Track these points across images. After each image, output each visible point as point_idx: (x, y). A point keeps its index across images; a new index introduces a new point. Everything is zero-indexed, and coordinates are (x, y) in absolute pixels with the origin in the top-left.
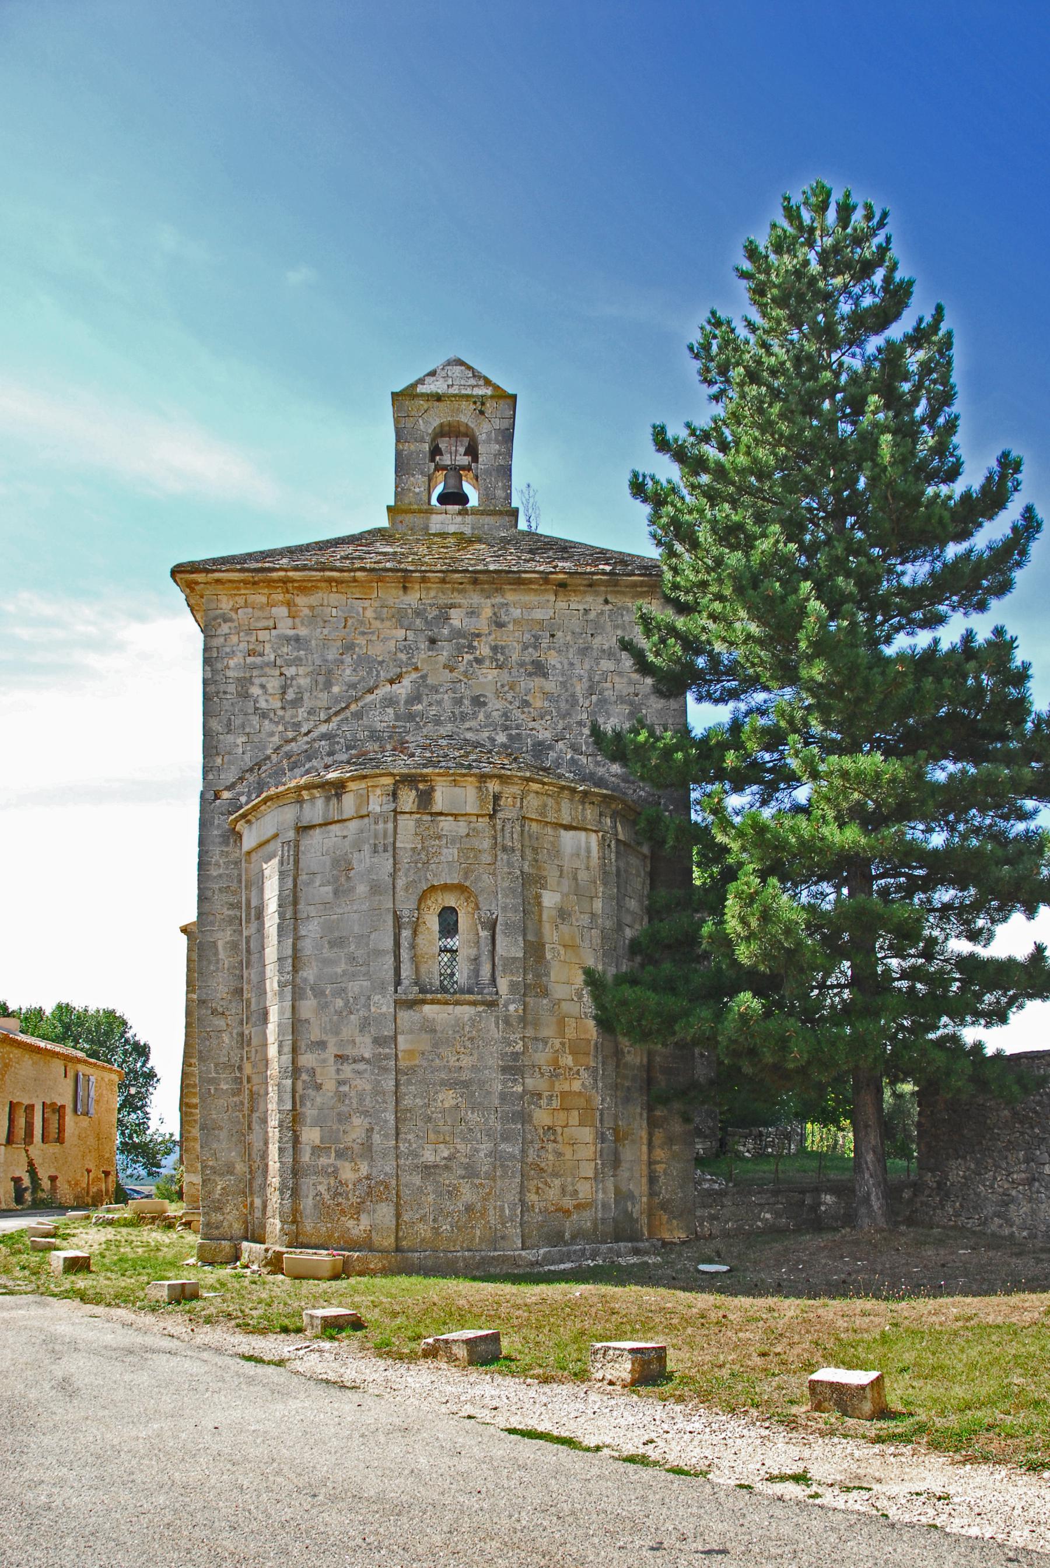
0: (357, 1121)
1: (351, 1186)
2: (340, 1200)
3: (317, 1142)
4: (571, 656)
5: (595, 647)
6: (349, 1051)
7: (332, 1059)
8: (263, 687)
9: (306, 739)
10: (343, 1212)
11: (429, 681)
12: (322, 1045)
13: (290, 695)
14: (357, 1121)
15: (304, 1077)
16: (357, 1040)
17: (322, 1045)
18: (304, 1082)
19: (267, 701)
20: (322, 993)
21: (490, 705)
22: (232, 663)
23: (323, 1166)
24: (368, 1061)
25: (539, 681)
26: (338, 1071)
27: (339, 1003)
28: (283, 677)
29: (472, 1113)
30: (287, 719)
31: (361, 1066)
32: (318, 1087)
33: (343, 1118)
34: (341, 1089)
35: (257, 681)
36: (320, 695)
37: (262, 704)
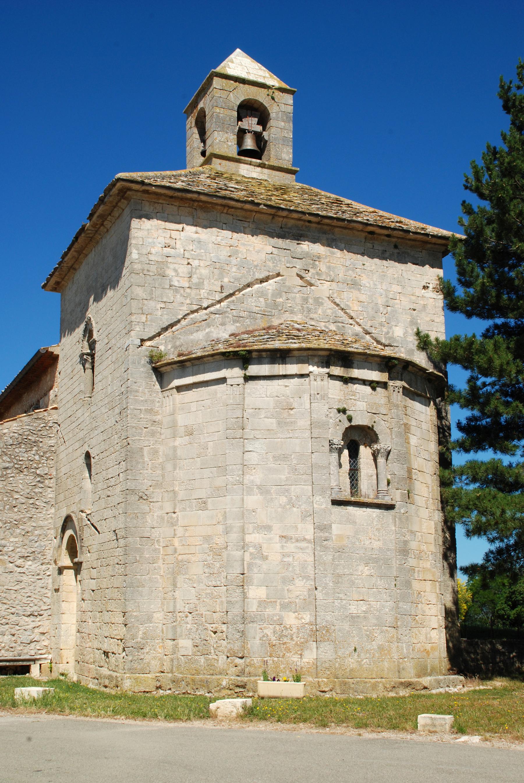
0: (299, 583)
1: (294, 630)
2: (285, 640)
3: (264, 596)
4: (375, 279)
5: (389, 275)
7: (277, 538)
8: (175, 270)
9: (204, 311)
10: (289, 650)
11: (287, 284)
12: (268, 528)
13: (195, 280)
14: (299, 583)
15: (251, 550)
16: (300, 526)
17: (268, 528)
18: (251, 554)
19: (178, 281)
20: (268, 492)
21: (325, 305)
22: (153, 251)
23: (268, 615)
24: (309, 541)
25: (355, 294)
26: (283, 547)
27: (283, 500)
28: (189, 266)
29: (381, 580)
30: (193, 295)
31: (304, 544)
32: (265, 558)
33: (288, 581)
34: (285, 560)
35: (172, 266)
36: (216, 283)
37: (176, 284)
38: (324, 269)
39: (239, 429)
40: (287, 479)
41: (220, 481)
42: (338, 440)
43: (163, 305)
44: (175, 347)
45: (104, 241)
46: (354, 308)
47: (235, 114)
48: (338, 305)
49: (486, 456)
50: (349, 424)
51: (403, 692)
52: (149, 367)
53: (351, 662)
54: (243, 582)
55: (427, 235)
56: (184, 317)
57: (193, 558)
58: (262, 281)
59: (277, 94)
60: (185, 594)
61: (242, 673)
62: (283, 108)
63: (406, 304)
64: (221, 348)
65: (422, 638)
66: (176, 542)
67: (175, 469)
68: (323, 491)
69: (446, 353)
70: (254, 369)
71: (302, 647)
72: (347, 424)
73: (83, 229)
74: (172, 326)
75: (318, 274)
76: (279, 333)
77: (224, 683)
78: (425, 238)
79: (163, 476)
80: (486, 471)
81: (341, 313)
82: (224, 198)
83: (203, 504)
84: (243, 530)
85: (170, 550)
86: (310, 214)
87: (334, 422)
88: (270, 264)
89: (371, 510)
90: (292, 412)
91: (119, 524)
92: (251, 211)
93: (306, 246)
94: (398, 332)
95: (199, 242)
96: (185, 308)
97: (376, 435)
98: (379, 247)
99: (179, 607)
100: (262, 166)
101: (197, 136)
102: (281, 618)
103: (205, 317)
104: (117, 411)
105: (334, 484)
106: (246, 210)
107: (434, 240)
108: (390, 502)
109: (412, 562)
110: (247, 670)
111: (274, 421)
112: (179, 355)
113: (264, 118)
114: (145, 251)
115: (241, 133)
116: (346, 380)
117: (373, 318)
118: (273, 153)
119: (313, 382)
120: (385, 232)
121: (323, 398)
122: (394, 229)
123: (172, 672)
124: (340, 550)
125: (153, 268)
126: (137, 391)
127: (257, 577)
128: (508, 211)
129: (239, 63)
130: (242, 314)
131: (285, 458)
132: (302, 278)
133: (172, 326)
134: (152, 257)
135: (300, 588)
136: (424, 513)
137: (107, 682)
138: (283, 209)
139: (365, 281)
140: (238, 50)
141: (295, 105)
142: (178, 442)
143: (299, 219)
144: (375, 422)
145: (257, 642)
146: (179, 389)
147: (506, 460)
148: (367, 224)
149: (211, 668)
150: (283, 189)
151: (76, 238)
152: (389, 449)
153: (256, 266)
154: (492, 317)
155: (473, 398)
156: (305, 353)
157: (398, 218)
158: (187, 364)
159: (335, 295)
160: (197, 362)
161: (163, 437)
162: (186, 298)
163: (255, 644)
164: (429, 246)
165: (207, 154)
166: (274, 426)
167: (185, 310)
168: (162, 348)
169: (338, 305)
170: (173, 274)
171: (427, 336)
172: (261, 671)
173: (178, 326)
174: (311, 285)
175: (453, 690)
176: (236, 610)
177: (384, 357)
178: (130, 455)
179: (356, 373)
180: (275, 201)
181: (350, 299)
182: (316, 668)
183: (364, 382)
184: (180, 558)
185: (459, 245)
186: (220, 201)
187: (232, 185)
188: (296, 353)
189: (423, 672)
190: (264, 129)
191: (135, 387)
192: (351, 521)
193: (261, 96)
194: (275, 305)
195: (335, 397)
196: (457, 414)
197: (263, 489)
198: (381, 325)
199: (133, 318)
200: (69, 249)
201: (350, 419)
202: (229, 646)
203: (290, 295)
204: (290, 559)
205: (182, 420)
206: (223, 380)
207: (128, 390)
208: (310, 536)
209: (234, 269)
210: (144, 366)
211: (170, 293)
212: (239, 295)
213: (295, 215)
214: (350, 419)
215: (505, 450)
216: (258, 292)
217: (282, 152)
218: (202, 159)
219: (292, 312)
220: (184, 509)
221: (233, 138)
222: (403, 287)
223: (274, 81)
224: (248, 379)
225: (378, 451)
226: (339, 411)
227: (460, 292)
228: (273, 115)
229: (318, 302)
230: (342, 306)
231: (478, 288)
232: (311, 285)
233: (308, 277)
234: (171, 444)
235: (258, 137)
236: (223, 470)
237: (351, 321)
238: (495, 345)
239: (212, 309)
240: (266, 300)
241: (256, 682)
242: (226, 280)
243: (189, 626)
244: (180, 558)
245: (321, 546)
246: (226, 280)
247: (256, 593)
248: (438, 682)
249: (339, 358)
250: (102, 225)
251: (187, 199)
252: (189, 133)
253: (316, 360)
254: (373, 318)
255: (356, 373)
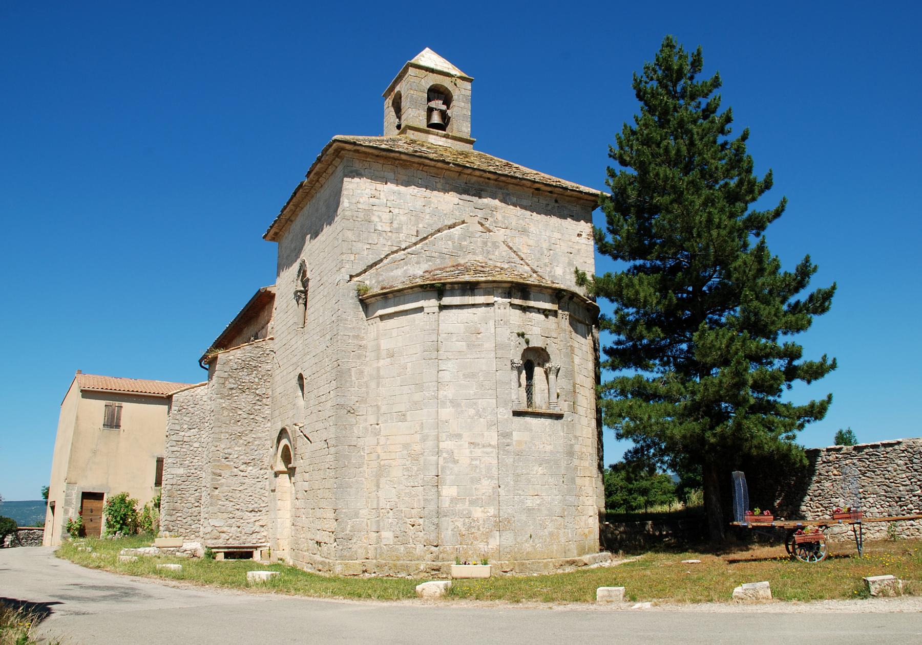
0: (485, 482)
1: (481, 522)
2: (473, 530)
3: (455, 494)
6: (477, 441)
8: (379, 217)
10: (476, 539)
12: (459, 436)
13: (395, 225)
14: (485, 482)
15: (445, 455)
16: (486, 434)
17: (459, 436)
18: (444, 458)
20: (459, 405)
22: (361, 200)
24: (494, 447)
25: (525, 238)
26: (471, 452)
27: (472, 412)
31: (489, 450)
32: (456, 462)
37: (380, 228)
38: (500, 218)
39: (434, 351)
40: (475, 394)
41: (417, 397)
42: (518, 361)
43: (368, 246)
44: (378, 282)
45: (318, 195)
46: (524, 251)
47: (426, 95)
48: (511, 248)
49: (630, 373)
51: (569, 569)
52: (357, 300)
53: (527, 547)
54: (438, 482)
55: (581, 192)
56: (386, 257)
57: (393, 463)
58: (450, 228)
59: (459, 81)
60: (387, 494)
61: (437, 558)
62: (463, 92)
63: (566, 250)
64: (419, 282)
65: (582, 524)
66: (379, 450)
67: (378, 386)
68: (505, 404)
69: (603, 288)
70: (446, 300)
71: (487, 536)
72: (525, 346)
73: (301, 186)
74: (375, 264)
75: (495, 222)
76: (467, 270)
77: (422, 567)
78: (580, 195)
79: (367, 393)
80: (632, 385)
81: (513, 255)
82: (421, 157)
83: (403, 417)
84: (438, 439)
85: (374, 456)
86: (490, 172)
88: (457, 213)
90: (479, 336)
91: (331, 434)
92: (442, 169)
93: (487, 201)
94: (559, 271)
95: (399, 194)
96: (386, 249)
97: (548, 355)
98: (543, 202)
99: (382, 505)
100: (447, 136)
101: (394, 114)
102: (470, 512)
103: (403, 257)
104: (328, 337)
105: (514, 397)
106: (438, 168)
107: (586, 197)
108: (560, 412)
109: (576, 462)
110: (441, 556)
111: (464, 343)
112: (382, 289)
113: (447, 98)
114: (354, 201)
115: (430, 111)
116: (525, 309)
117: (539, 260)
118: (455, 126)
119: (497, 310)
120: (549, 189)
121: (505, 323)
122: (556, 186)
123: (376, 558)
124: (519, 454)
125: (361, 215)
126: (346, 320)
127: (449, 478)
128: (648, 172)
129: (428, 58)
130: (434, 254)
131: (473, 375)
132: (482, 225)
133: (375, 264)
134: (360, 206)
135: (486, 487)
136: (584, 421)
137: (320, 567)
138: (468, 168)
139: (532, 229)
140: (427, 49)
141: (472, 90)
142: (382, 362)
143: (481, 177)
145: (450, 532)
146: (382, 317)
147: (647, 375)
148: (535, 182)
149: (410, 555)
150: (466, 155)
151: (295, 193)
153: (445, 214)
154: (634, 259)
155: (622, 325)
156: (490, 285)
157: (558, 179)
158: (389, 296)
159: (509, 240)
160: (398, 294)
161: (367, 359)
162: (387, 240)
163: (447, 534)
164: (582, 201)
165: (402, 127)
166: (464, 348)
167: (387, 250)
168: (367, 282)
169: (511, 248)
170: (377, 220)
171: (584, 274)
172: (453, 556)
173: (381, 264)
174: (490, 231)
175: (606, 564)
176: (432, 507)
177: (555, 289)
178: (341, 375)
179: (532, 303)
180: (460, 161)
181: (521, 244)
182: (499, 553)
183: (539, 311)
184: (382, 463)
185: (607, 201)
186: (417, 160)
187: (424, 149)
188: (483, 285)
189: (582, 551)
190: (448, 108)
191: (344, 316)
192: (528, 429)
193: (446, 82)
194: (461, 247)
196: (607, 339)
197: (454, 403)
198: (546, 265)
199: (344, 257)
200: (288, 203)
201: (527, 342)
202: (425, 537)
203: (473, 240)
204: (478, 462)
205: (385, 344)
206: (421, 309)
207: (339, 319)
208: (494, 442)
209: (427, 217)
210: (352, 298)
211: (375, 236)
212: (431, 239)
213: (477, 173)
214: (527, 342)
215: (646, 368)
216: (447, 236)
217: (462, 125)
218: (398, 131)
219: (474, 254)
220: (386, 421)
221: (423, 114)
222: (563, 234)
223: (455, 71)
224: (442, 308)
225: (550, 368)
226: (519, 335)
227: (609, 239)
228: (455, 97)
229: (495, 245)
230: (515, 249)
231: (624, 235)
232: (490, 231)
233: (487, 224)
234: (375, 365)
235: (443, 114)
236: (420, 386)
237: (521, 262)
238: (639, 280)
239: (409, 250)
240: (454, 243)
241: (449, 566)
242: (421, 226)
243: (390, 520)
244: (382, 463)
245: (504, 450)
246: (421, 226)
247: (449, 491)
248: (595, 559)
249: (519, 291)
250: (318, 181)
251: (390, 158)
252: (386, 112)
253: (500, 291)
254: (539, 260)
255: (532, 303)
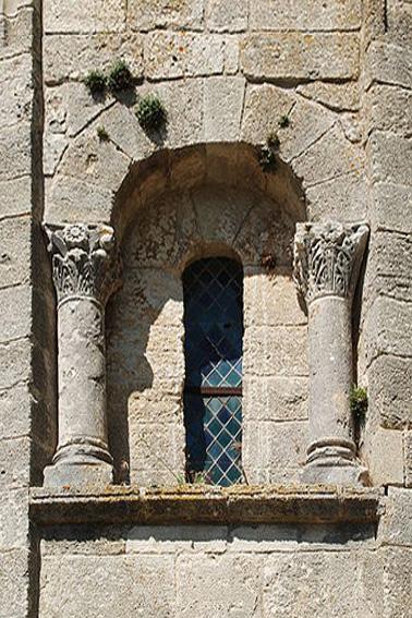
50: (152, 147)
72: (138, 147)
87: (72, 143)
89: (253, 545)
144: (285, 123)
152: (356, 237)
195: (76, 26)
201: (154, 120)
214: (154, 120)
226: (96, 87)
